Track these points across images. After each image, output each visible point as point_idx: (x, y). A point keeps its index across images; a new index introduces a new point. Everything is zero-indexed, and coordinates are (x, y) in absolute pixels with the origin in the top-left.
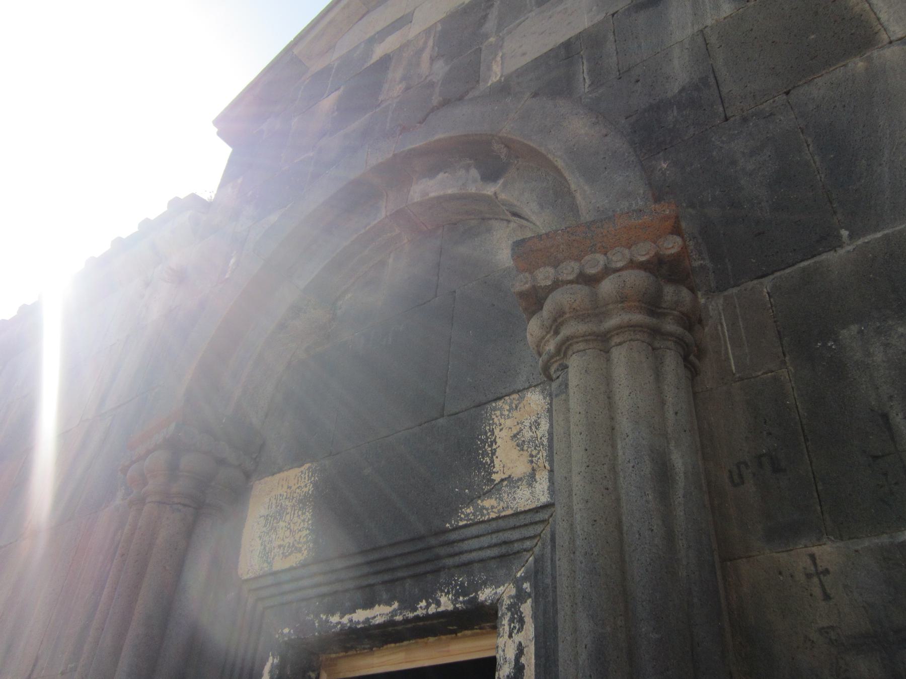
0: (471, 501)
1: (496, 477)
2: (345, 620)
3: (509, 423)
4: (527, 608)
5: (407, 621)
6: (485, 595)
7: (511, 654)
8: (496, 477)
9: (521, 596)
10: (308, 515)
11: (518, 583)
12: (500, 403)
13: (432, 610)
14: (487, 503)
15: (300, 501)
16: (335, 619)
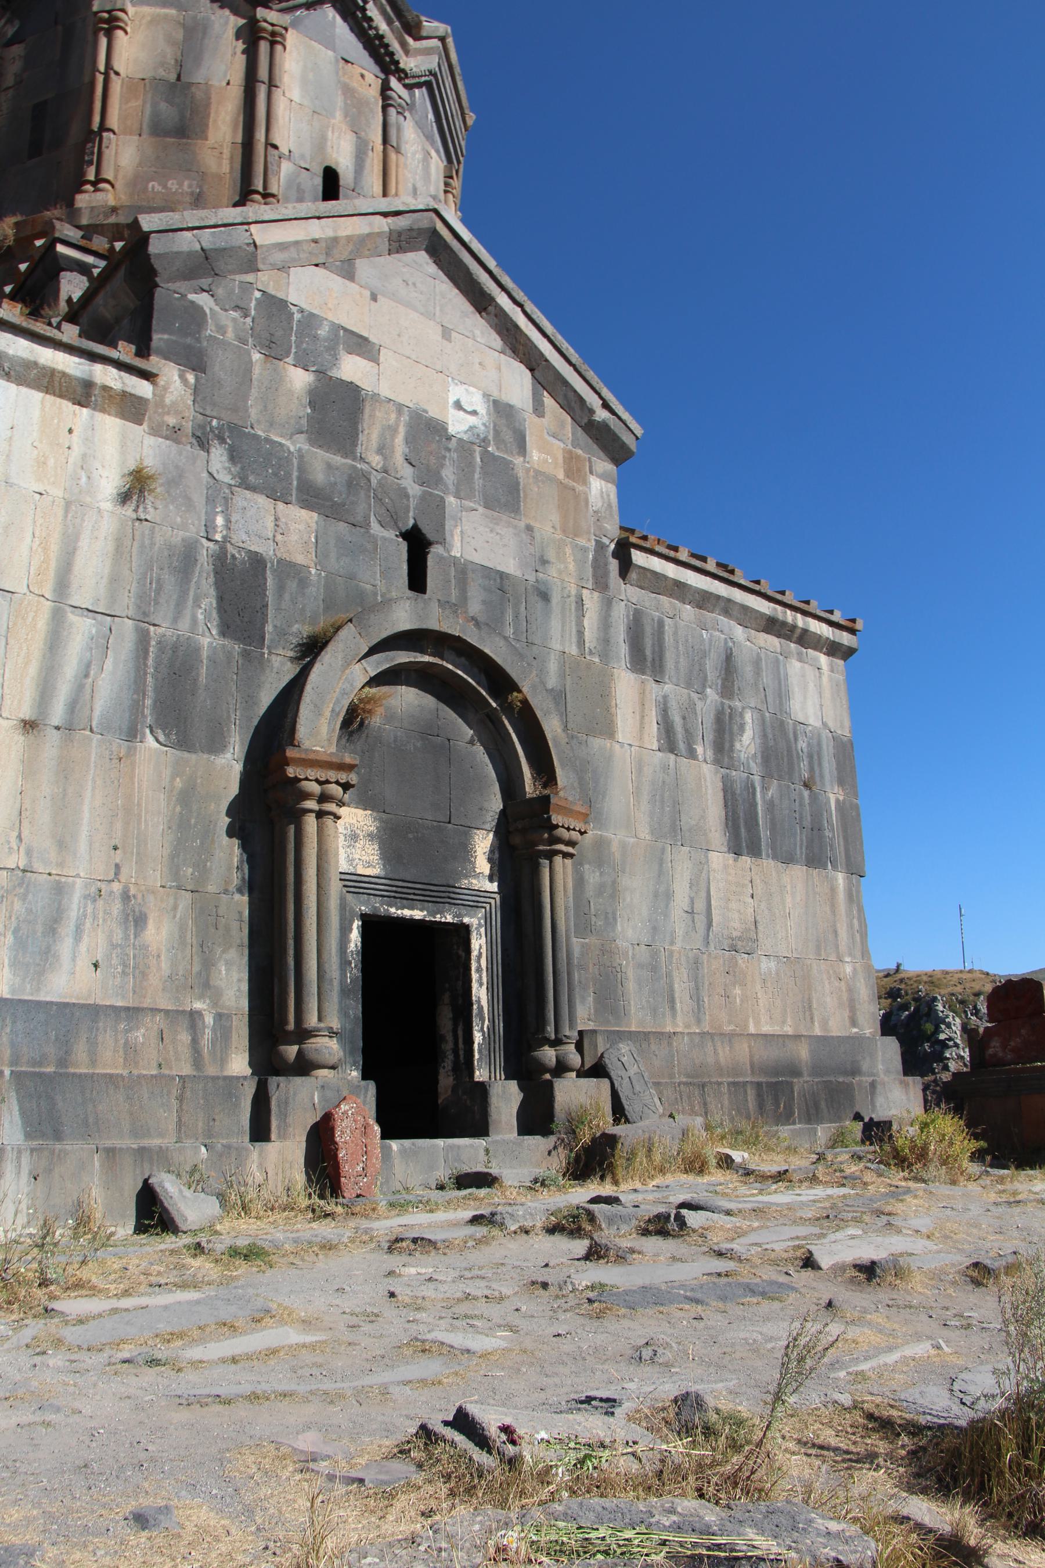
0: (466, 877)
1: (478, 871)
2: (399, 912)
3: (482, 845)
4: (483, 930)
5: (430, 921)
6: (466, 920)
7: (477, 947)
8: (478, 871)
9: (479, 924)
10: (376, 847)
11: (479, 919)
12: (478, 832)
13: (443, 920)
14: (474, 881)
15: (369, 835)
16: (393, 910)
